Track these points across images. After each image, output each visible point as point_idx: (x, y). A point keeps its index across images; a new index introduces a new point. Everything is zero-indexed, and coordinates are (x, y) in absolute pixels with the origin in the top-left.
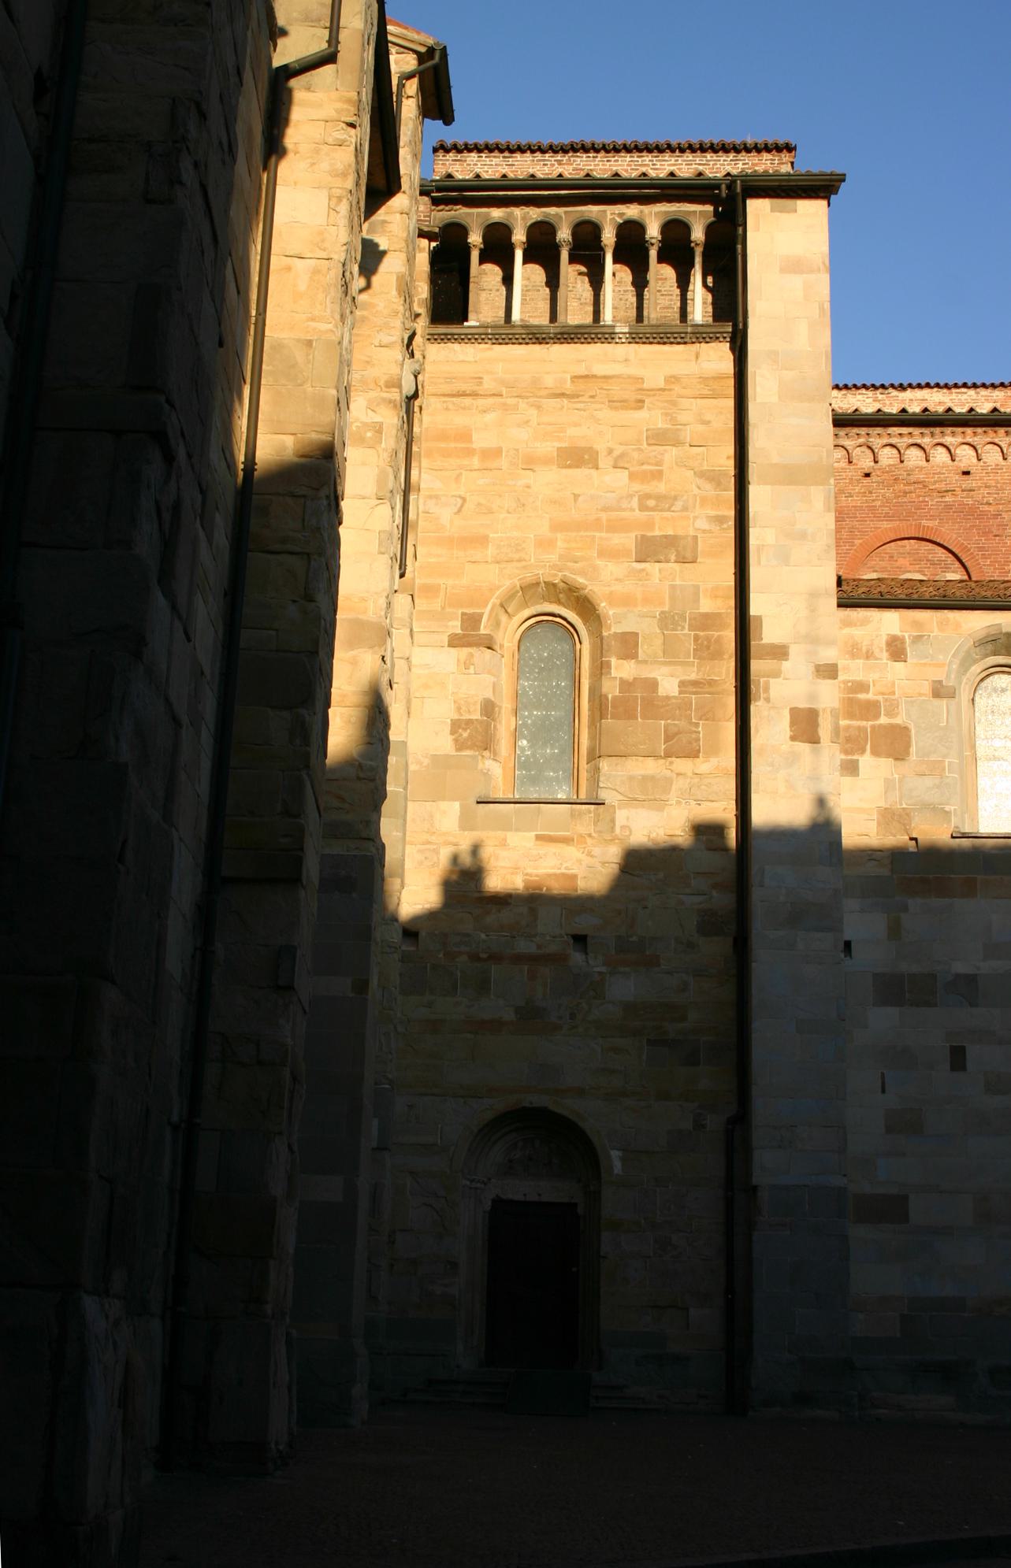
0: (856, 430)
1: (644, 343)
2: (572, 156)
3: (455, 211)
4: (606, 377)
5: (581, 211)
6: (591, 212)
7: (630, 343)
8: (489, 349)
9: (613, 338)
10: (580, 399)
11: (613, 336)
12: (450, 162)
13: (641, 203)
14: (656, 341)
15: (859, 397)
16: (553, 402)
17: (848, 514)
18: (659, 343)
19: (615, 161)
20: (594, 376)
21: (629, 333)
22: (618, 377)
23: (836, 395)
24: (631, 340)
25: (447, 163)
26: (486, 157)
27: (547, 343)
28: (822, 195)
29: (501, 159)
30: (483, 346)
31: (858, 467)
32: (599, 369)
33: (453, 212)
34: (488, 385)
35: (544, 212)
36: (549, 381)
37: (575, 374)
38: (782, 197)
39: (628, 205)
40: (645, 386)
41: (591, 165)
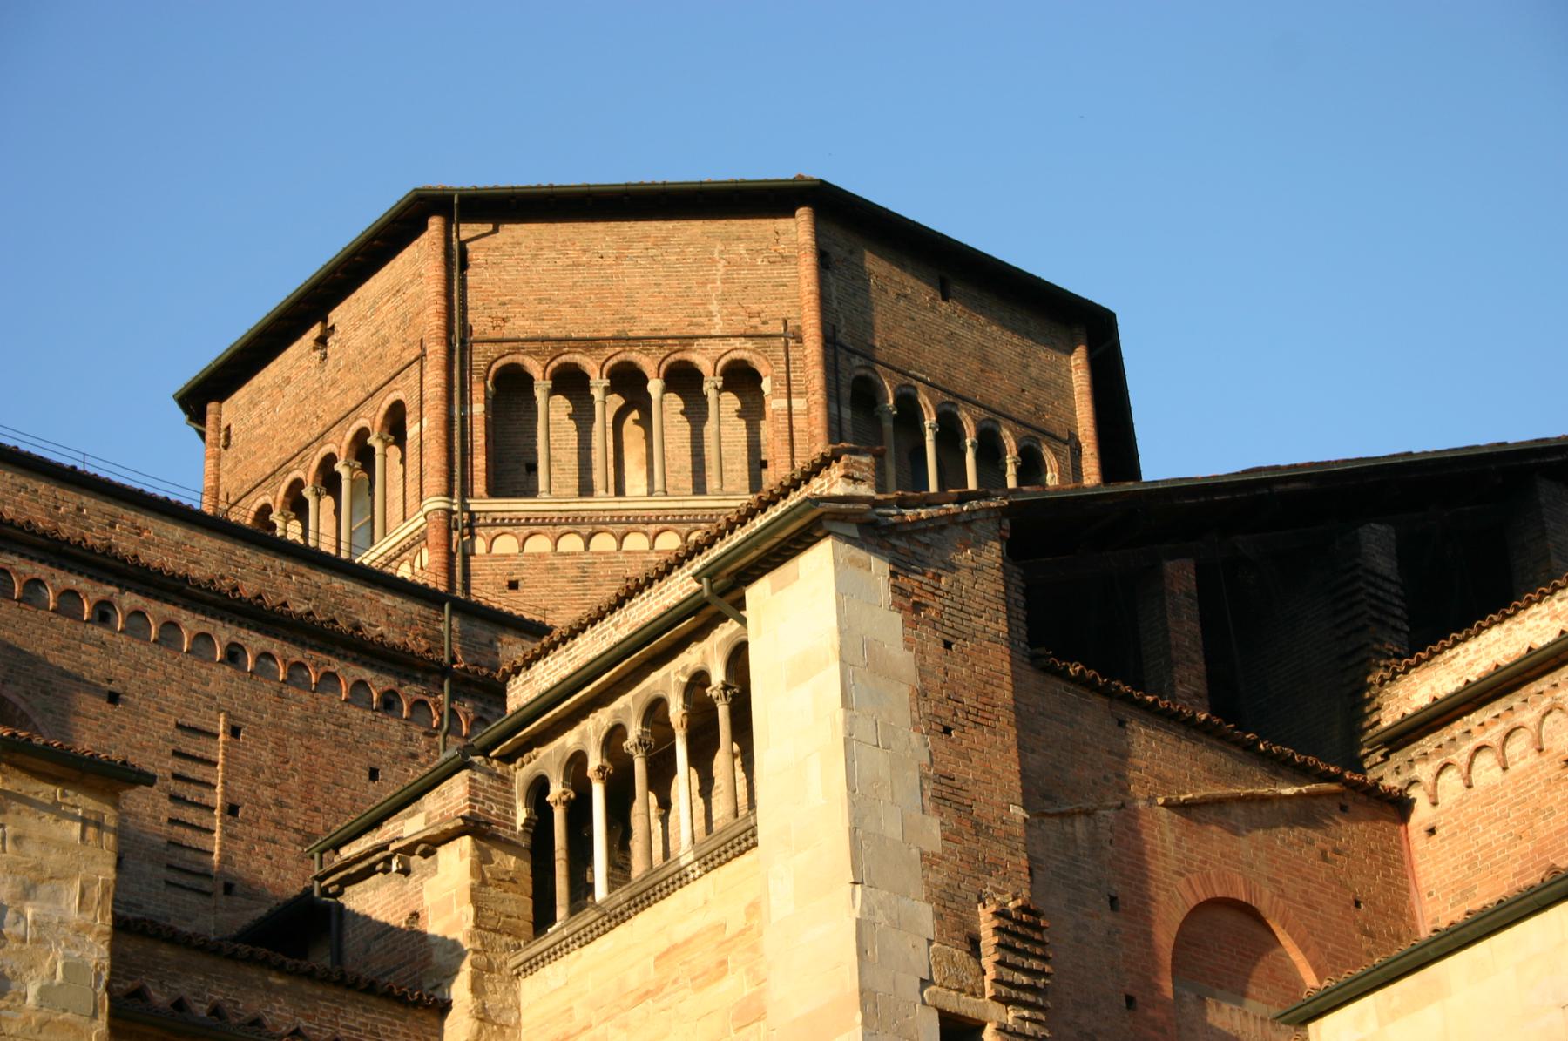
0: (1534, 687)
1: (721, 864)
2: (629, 607)
3: (535, 758)
4: (687, 942)
5: (648, 688)
6: (656, 682)
7: (707, 872)
8: (580, 956)
9: (687, 875)
10: (666, 991)
11: (683, 872)
12: (522, 688)
13: (700, 640)
14: (730, 854)
15: (1530, 623)
16: (639, 1011)
17: (1553, 849)
18: (735, 856)
19: (668, 589)
20: (675, 947)
21: (698, 859)
22: (696, 936)
23: (1497, 637)
24: (704, 868)
25: (518, 691)
26: (552, 660)
27: (630, 917)
28: (819, 534)
29: (565, 654)
30: (573, 954)
31: (1555, 752)
32: (680, 933)
33: (534, 761)
34: (580, 1015)
35: (614, 711)
36: (634, 980)
37: (657, 954)
38: (782, 563)
39: (687, 650)
40: (728, 934)
41: (645, 611)
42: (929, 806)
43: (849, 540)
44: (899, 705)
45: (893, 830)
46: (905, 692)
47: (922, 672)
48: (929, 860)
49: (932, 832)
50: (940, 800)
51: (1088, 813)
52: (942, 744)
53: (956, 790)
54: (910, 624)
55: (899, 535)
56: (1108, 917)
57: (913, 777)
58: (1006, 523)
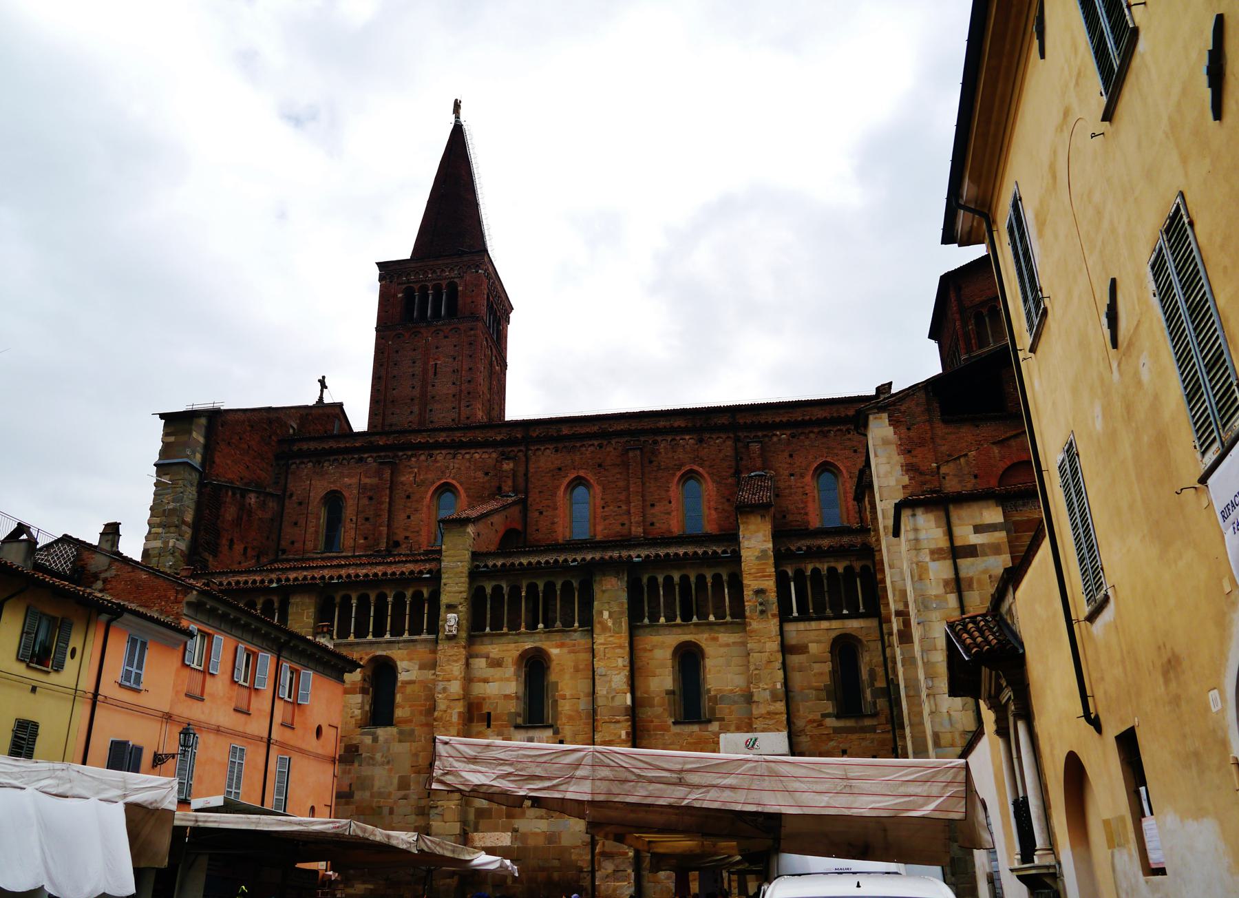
42: (904, 473)
43: (875, 413)
44: (893, 450)
45: (892, 482)
46: (894, 447)
47: (900, 439)
48: (904, 487)
49: (906, 480)
50: (907, 471)
51: (966, 455)
52: (907, 456)
53: (913, 466)
54: (895, 427)
55: (890, 406)
56: (974, 481)
57: (899, 468)
58: (930, 388)
